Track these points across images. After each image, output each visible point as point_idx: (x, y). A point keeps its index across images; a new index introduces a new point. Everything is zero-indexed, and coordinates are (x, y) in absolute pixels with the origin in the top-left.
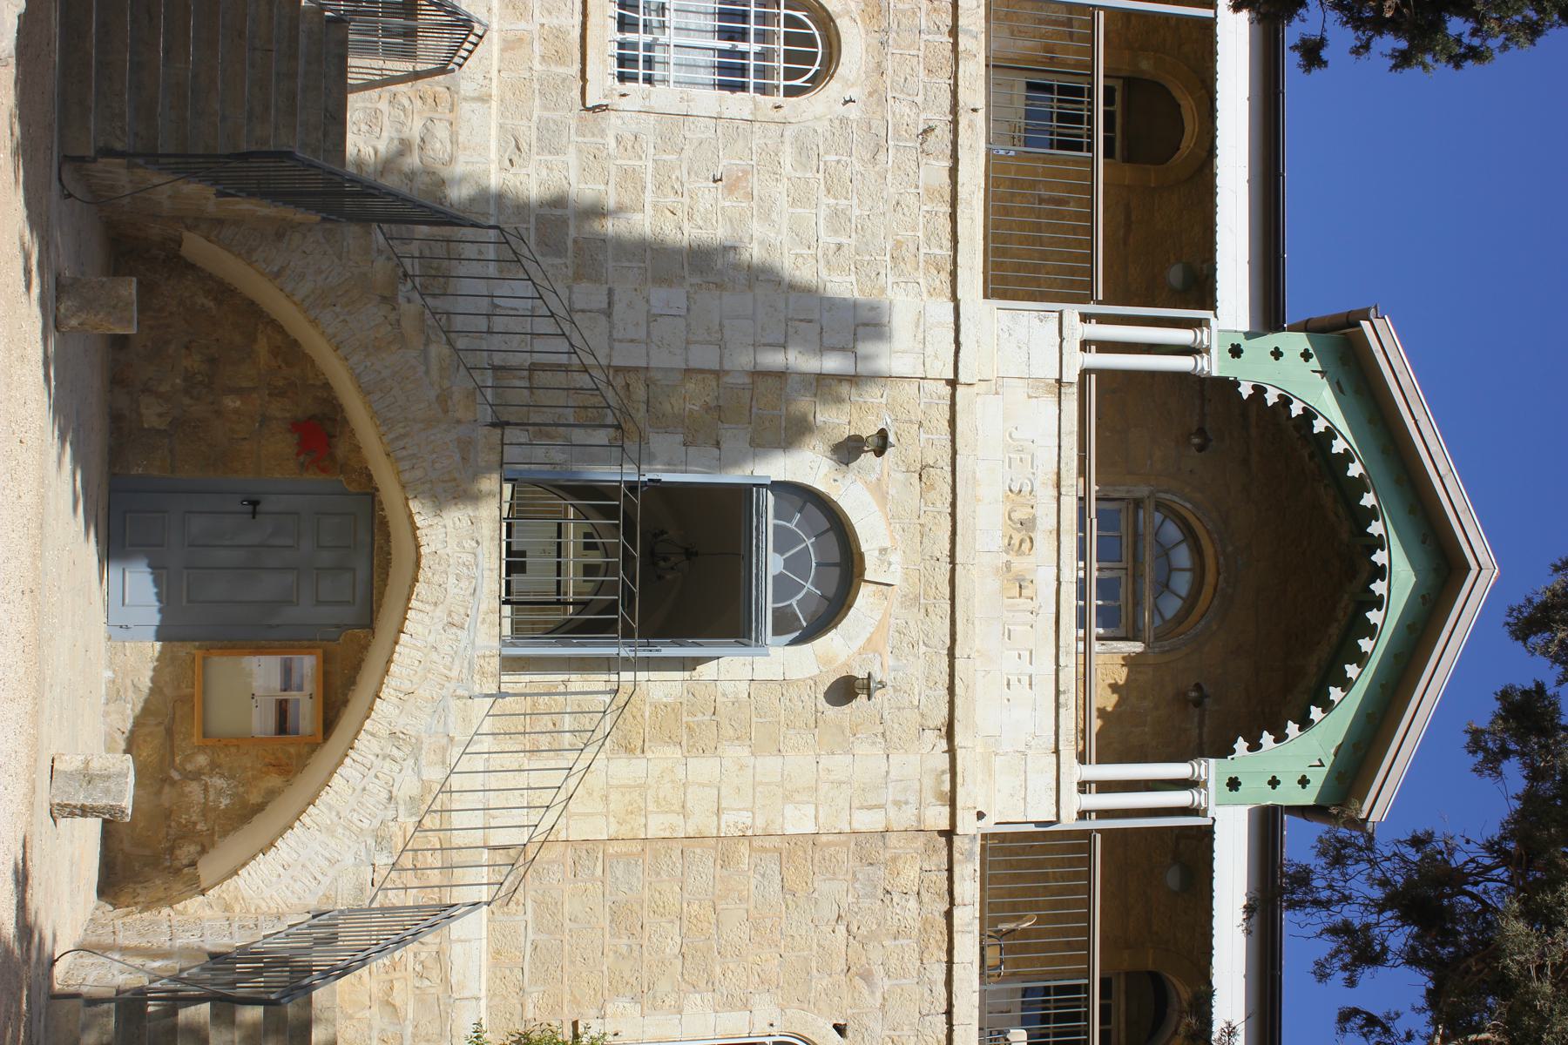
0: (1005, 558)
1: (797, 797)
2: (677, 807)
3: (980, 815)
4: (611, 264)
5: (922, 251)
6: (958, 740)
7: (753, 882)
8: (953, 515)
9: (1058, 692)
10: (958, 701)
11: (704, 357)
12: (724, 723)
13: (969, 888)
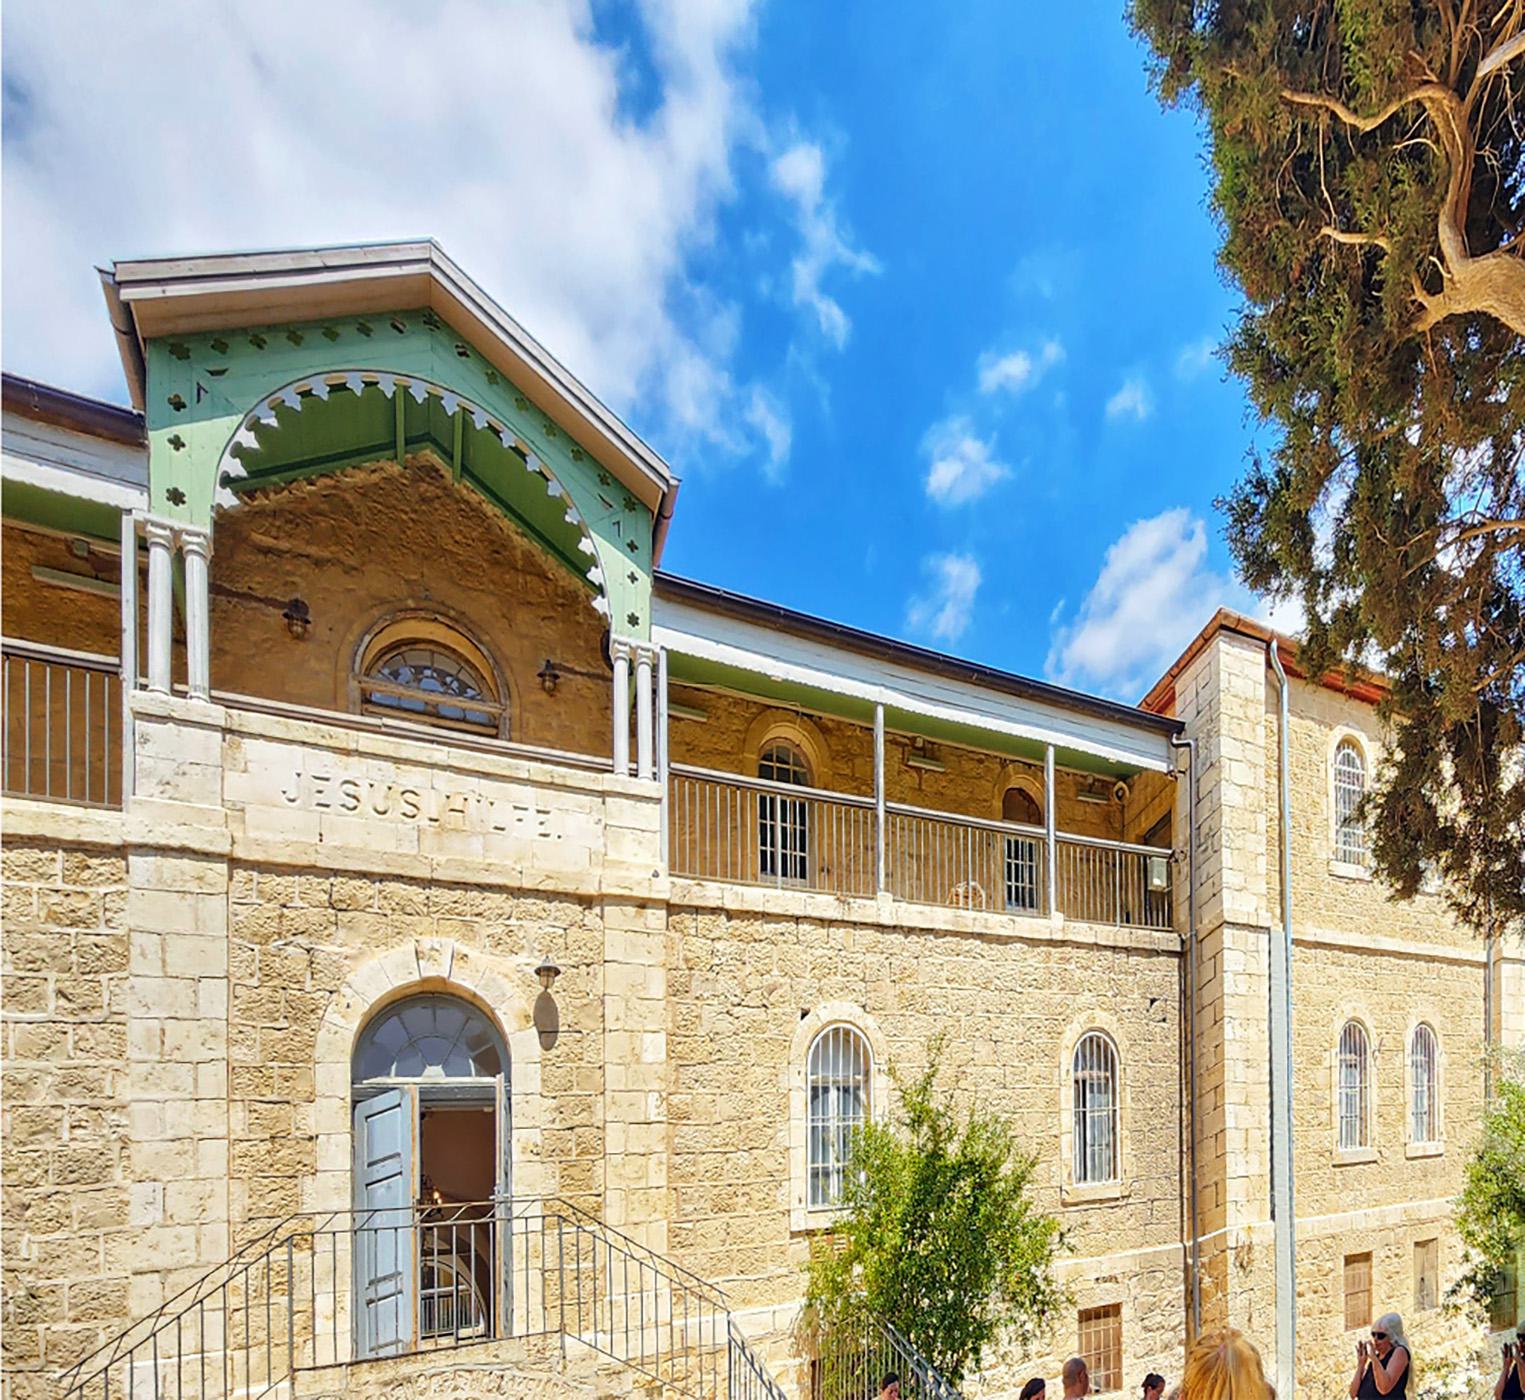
3: (656, 875)
4: (103, 1275)
6: (590, 889)
7: (701, 1090)
8: (383, 878)
9: (551, 786)
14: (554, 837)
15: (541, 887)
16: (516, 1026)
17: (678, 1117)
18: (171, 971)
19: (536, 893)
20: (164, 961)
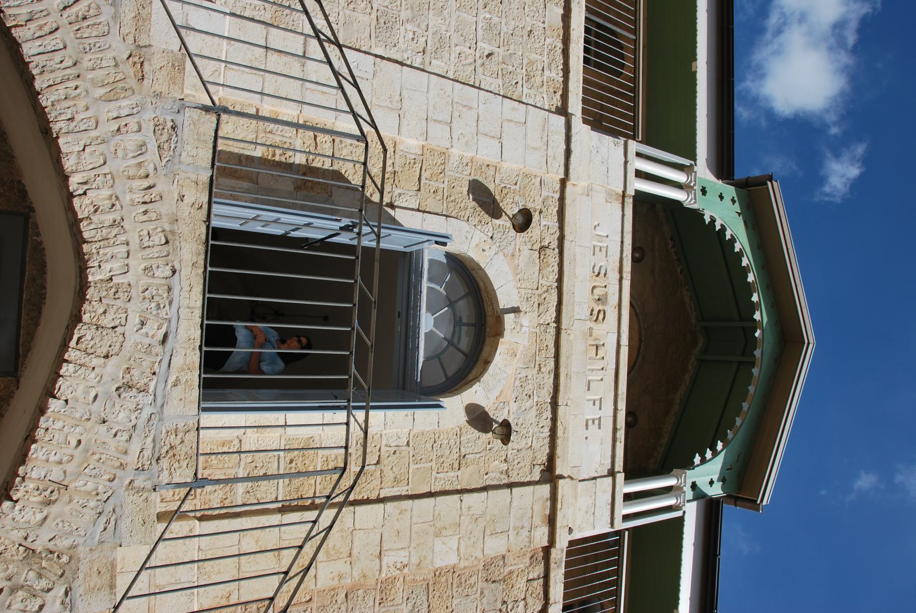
1: (444, 533)
2: (345, 554)
5: (547, 73)
10: (559, 442)
12: (387, 470)
14: (586, 434)
15: (559, 423)
18: (505, 124)
19: (554, 420)
20: (511, 121)
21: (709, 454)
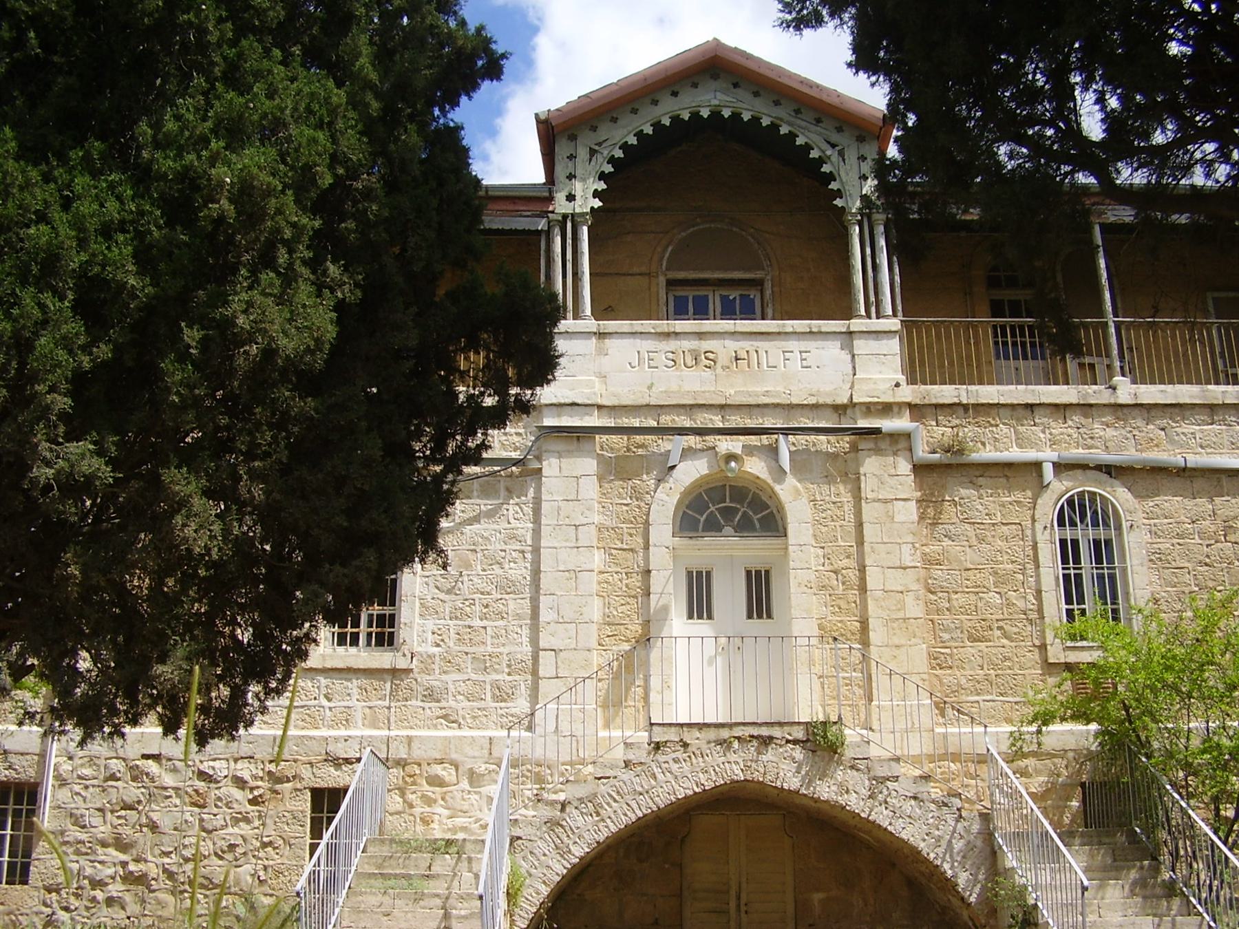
0: (719, 370)
3: (897, 385)
11: (591, 582)
13: (946, 393)
16: (791, 499)
17: (930, 562)
21: (834, 186)
